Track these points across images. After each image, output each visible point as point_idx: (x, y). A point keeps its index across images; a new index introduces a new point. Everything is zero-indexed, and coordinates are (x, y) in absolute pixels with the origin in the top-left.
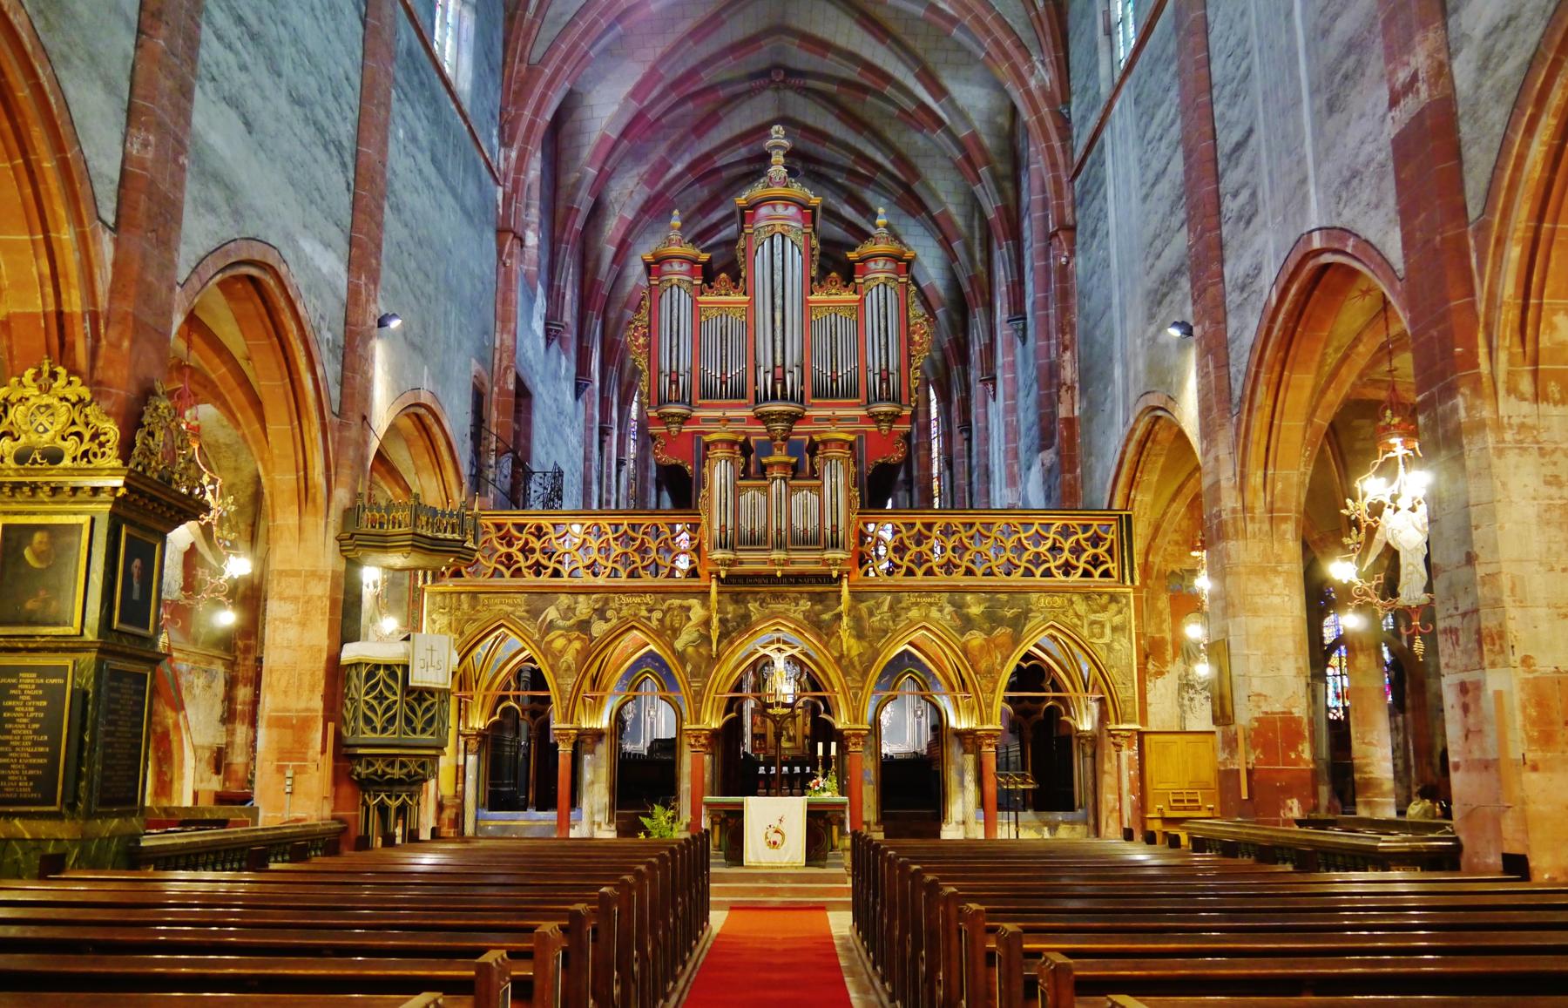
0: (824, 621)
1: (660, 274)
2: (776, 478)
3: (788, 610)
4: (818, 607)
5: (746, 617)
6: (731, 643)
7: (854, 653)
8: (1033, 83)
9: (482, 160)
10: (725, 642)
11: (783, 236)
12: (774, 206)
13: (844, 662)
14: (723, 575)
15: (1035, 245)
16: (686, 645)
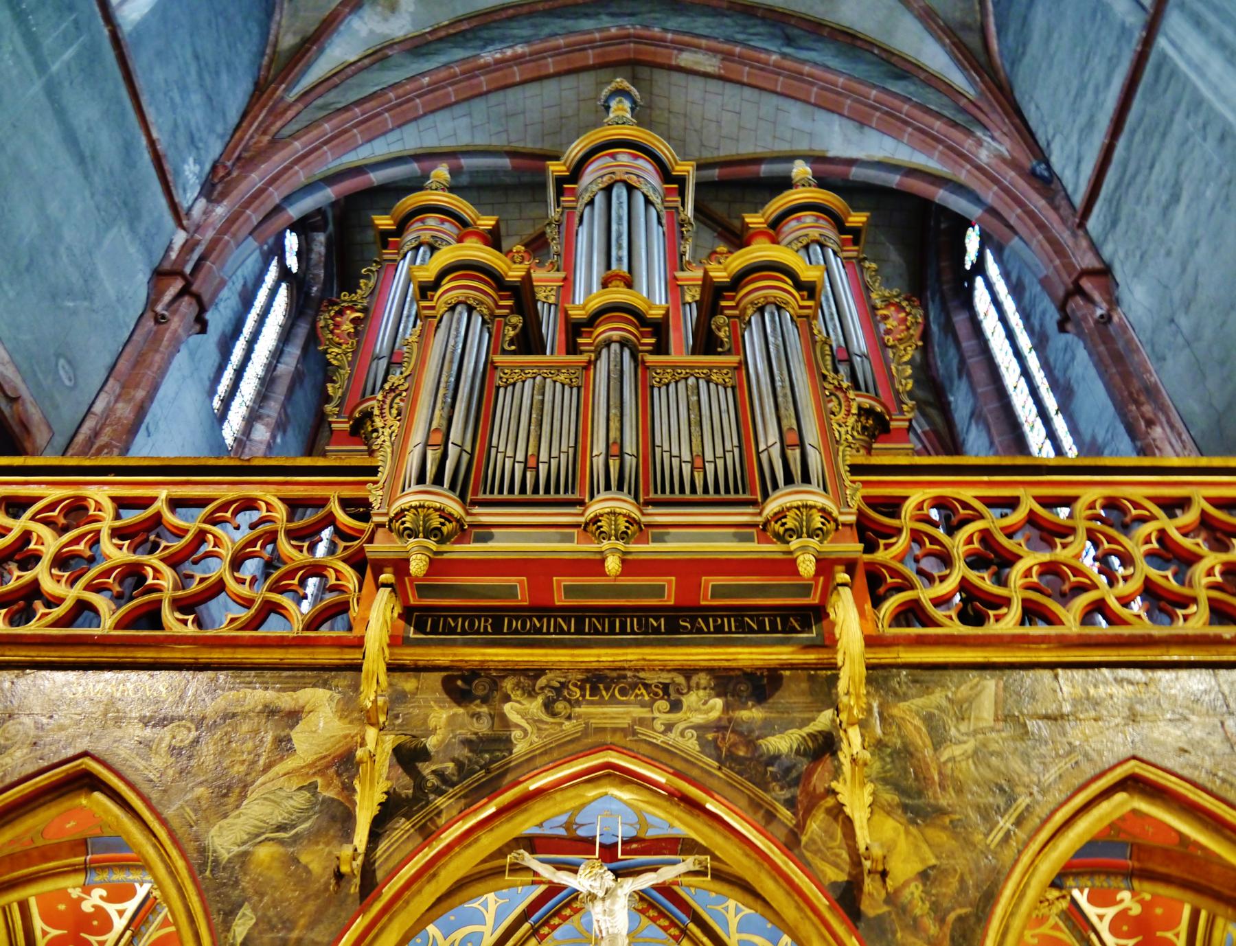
0: (774, 758)
1: (397, 246)
2: (608, 343)
3: (641, 721)
4: (752, 714)
5: (499, 742)
6: (427, 833)
7: (903, 868)
8: (984, 156)
9: (144, 141)
10: (402, 827)
11: (631, 189)
12: (613, 156)
13: (873, 903)
14: (418, 566)
15: (997, 440)
16: (256, 837)
